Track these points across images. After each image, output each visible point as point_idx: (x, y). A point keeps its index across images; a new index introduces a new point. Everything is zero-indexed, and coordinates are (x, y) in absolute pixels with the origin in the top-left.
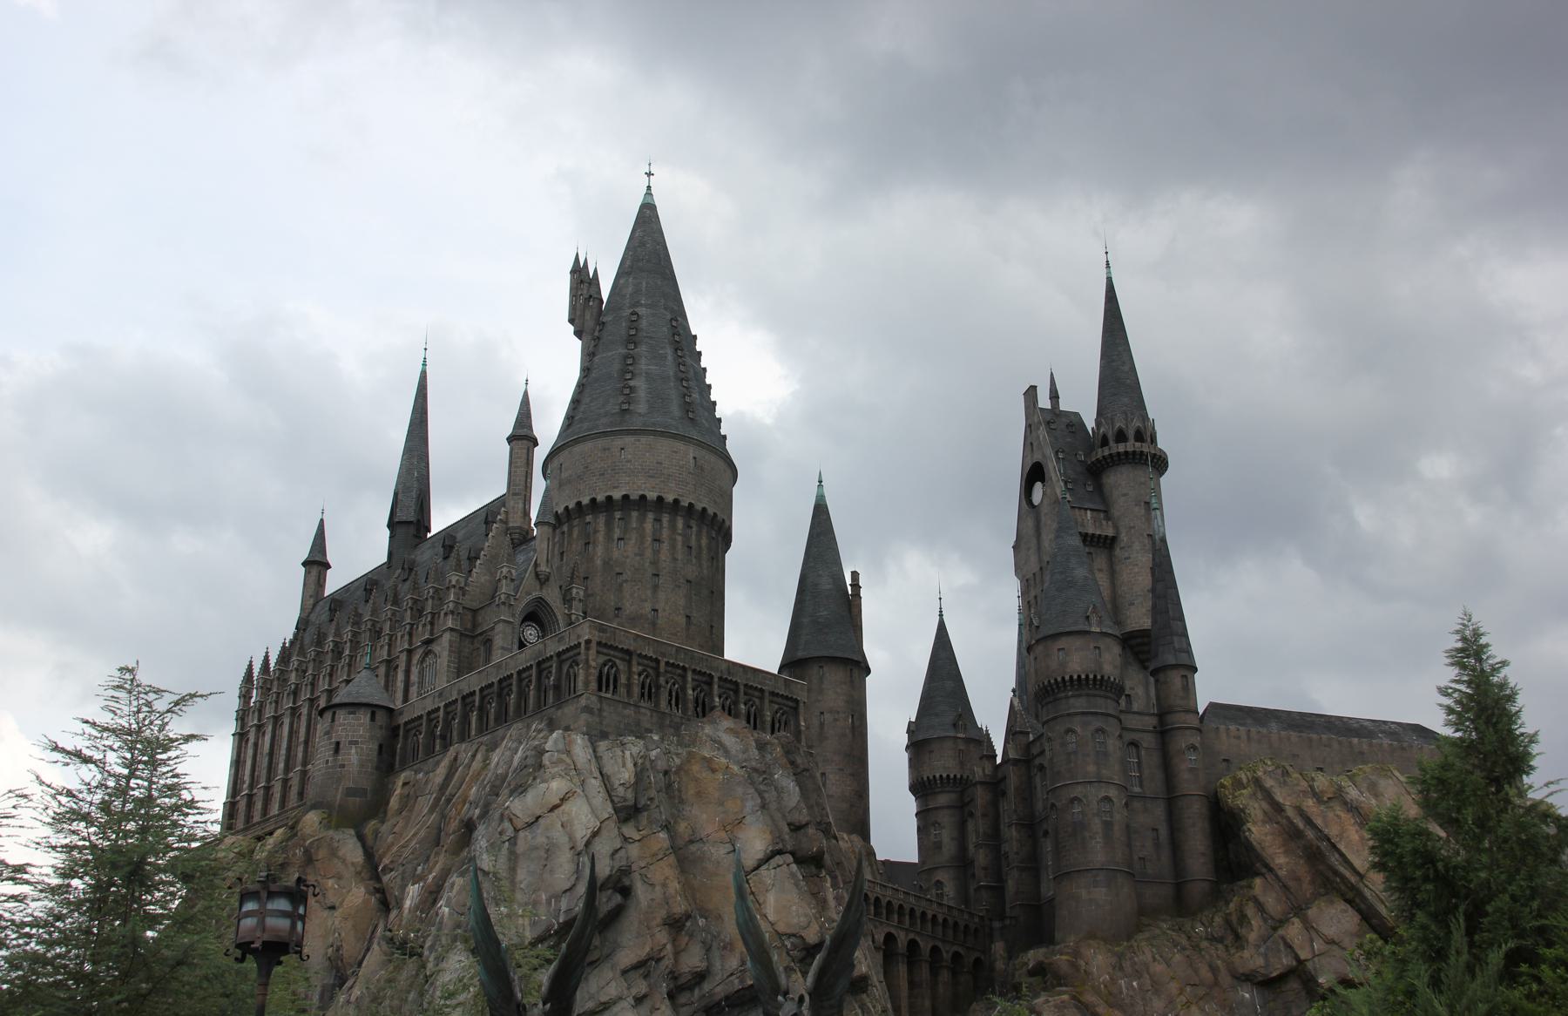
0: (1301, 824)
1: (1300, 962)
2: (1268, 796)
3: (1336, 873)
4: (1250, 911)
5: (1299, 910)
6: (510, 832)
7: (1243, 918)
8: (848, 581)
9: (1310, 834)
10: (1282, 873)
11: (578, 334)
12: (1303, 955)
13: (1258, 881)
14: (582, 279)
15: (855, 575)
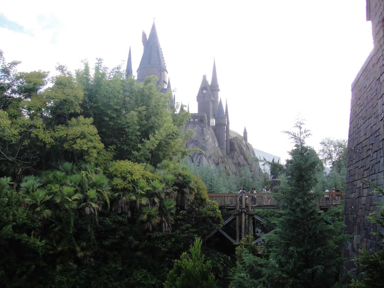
0: (240, 146)
1: (239, 162)
2: (237, 141)
3: (243, 152)
4: (235, 155)
5: (239, 156)
6: (205, 142)
7: (234, 156)
8: (173, 96)
9: (241, 147)
10: (238, 151)
11: (144, 45)
12: (240, 161)
13: (235, 152)
14: (144, 35)
15: (174, 95)
